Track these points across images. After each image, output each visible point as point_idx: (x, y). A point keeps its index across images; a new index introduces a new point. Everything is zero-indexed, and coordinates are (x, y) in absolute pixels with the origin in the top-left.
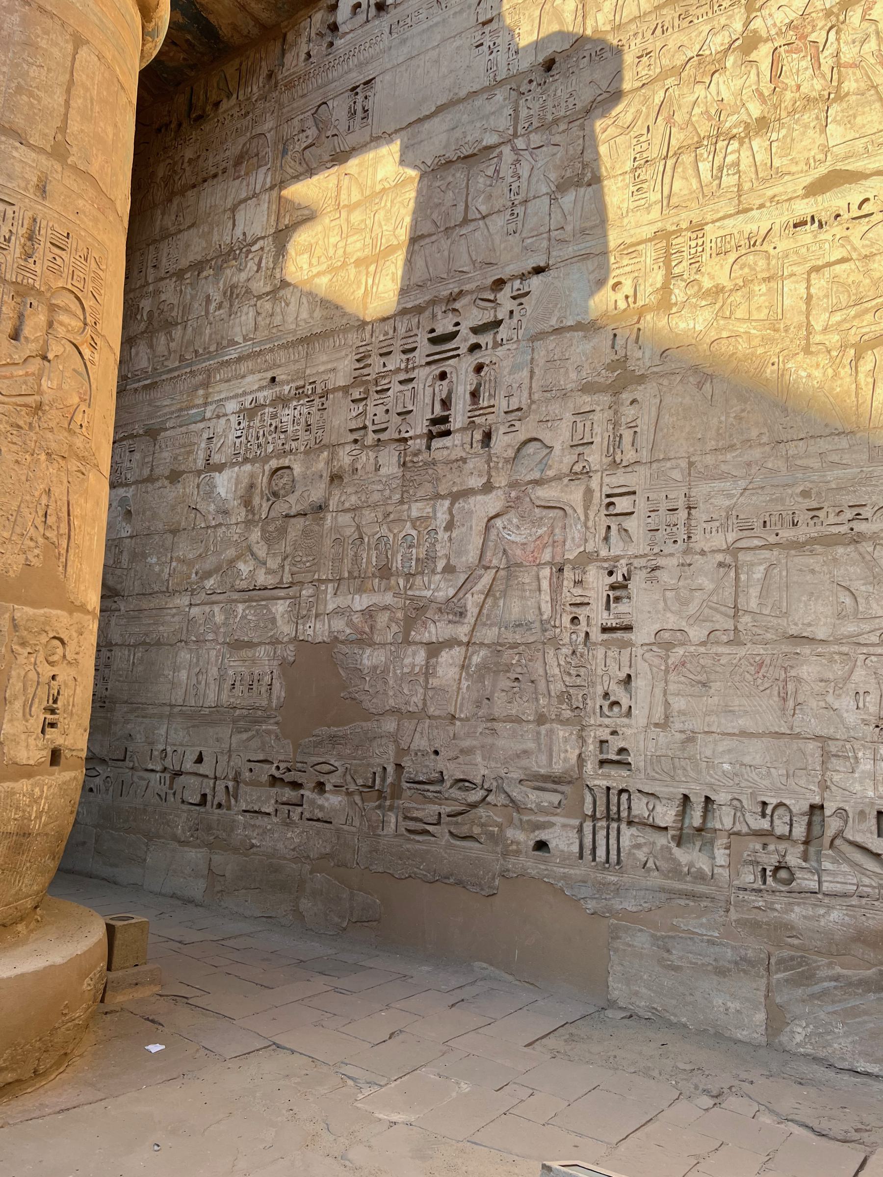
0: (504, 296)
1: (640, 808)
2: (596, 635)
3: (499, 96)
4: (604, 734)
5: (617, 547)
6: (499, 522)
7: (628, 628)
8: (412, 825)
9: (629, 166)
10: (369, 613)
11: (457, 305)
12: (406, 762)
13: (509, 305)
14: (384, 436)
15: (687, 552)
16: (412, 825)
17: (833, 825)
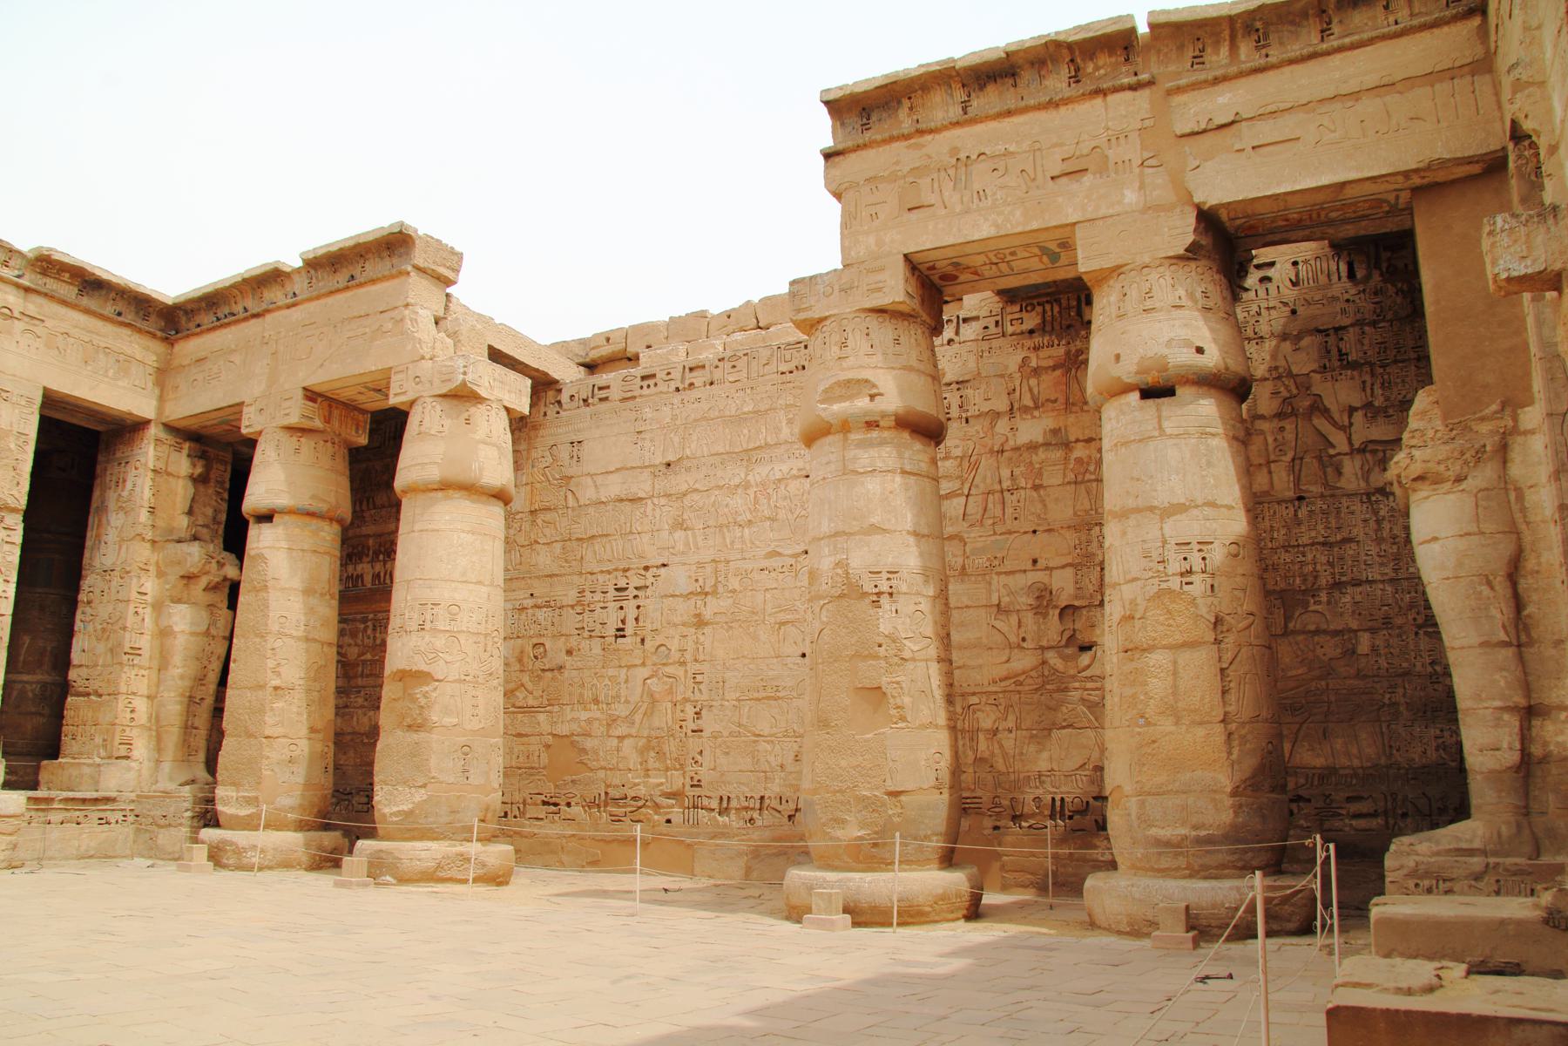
0: (649, 574)
1: (706, 802)
2: (690, 734)
3: (647, 472)
4: (693, 774)
5: (698, 696)
6: (648, 681)
7: (701, 731)
8: (613, 818)
9: (701, 526)
10: (589, 721)
11: (628, 574)
12: (609, 790)
13: (652, 580)
14: (593, 634)
15: (722, 699)
16: (613, 818)
17: (767, 802)
